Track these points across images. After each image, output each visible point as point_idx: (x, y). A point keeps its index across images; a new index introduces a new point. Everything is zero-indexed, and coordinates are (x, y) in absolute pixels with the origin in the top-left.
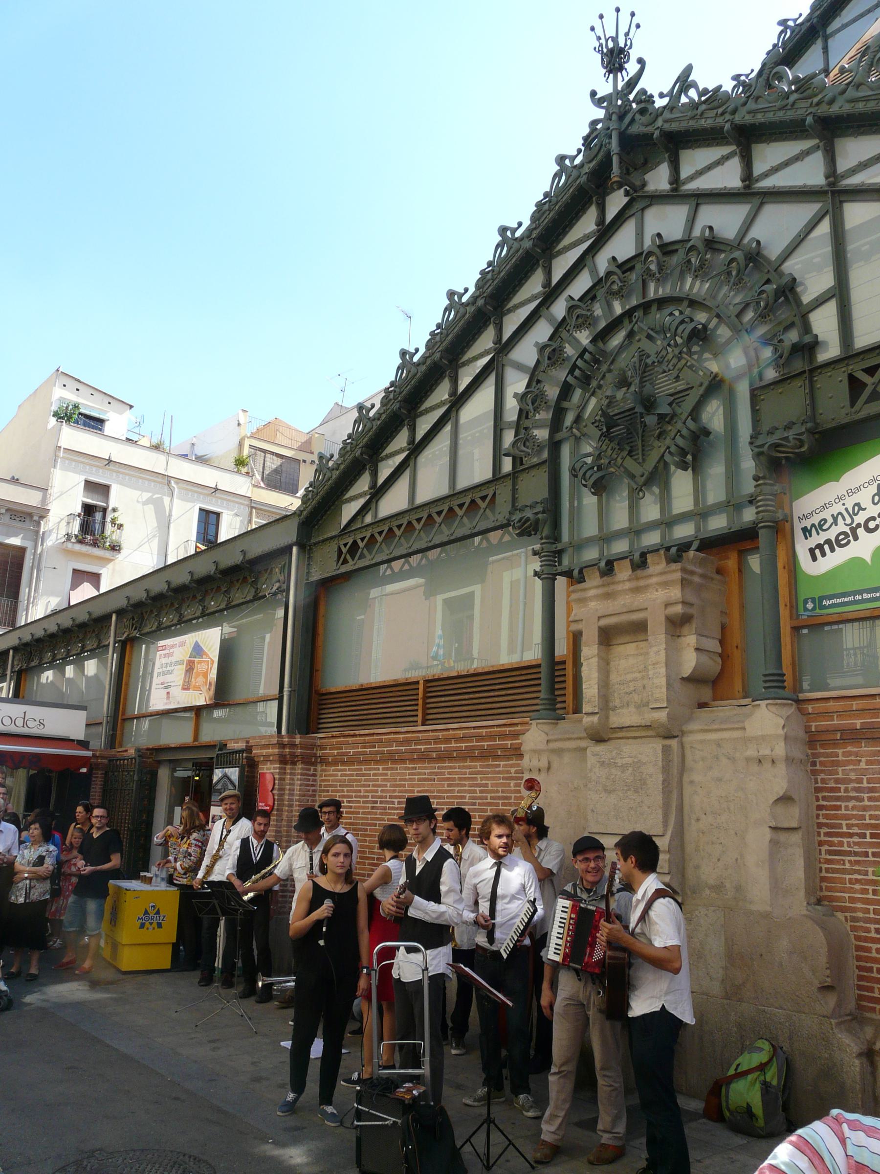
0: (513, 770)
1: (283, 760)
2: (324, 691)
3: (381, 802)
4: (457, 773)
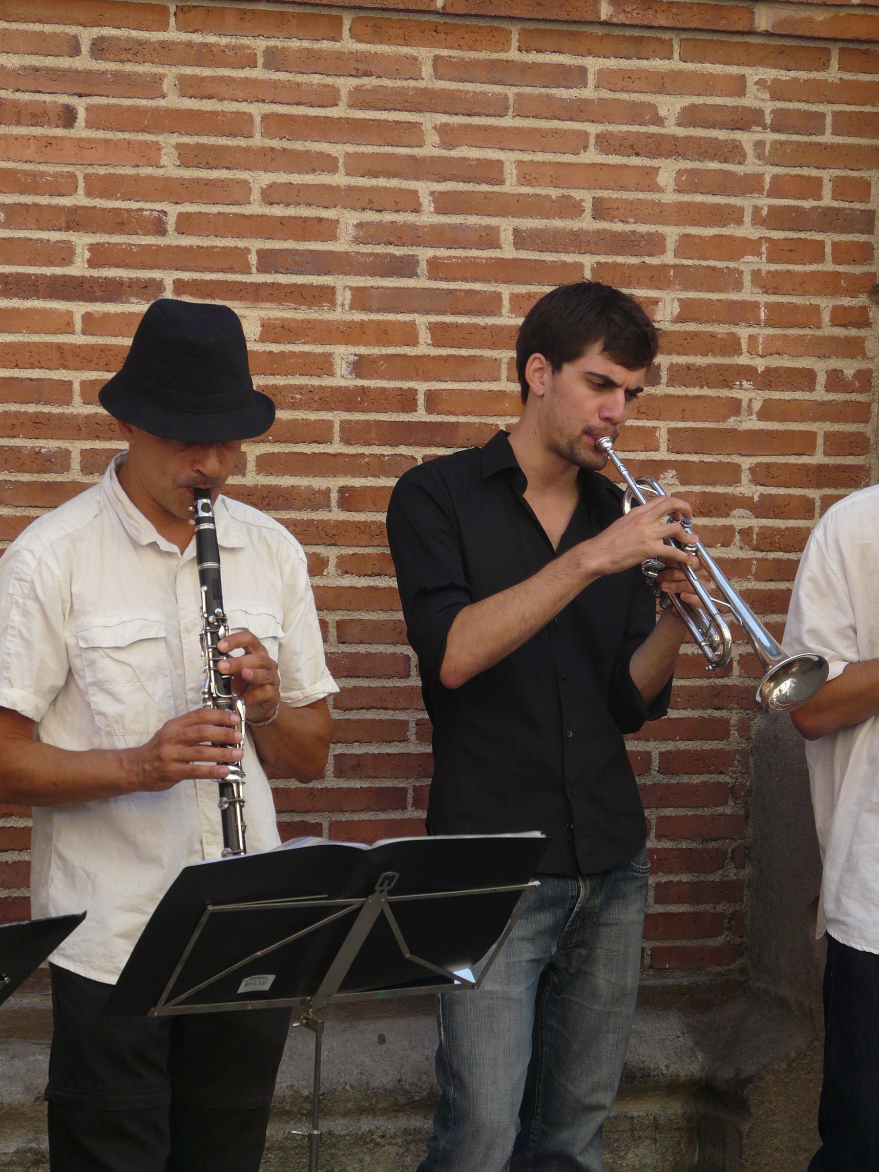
0: (670, 106)
4: (255, 91)
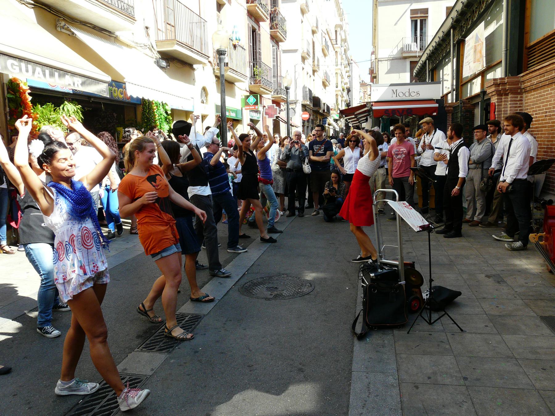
1: (499, 94)
2: (528, 45)
3: (549, 112)
